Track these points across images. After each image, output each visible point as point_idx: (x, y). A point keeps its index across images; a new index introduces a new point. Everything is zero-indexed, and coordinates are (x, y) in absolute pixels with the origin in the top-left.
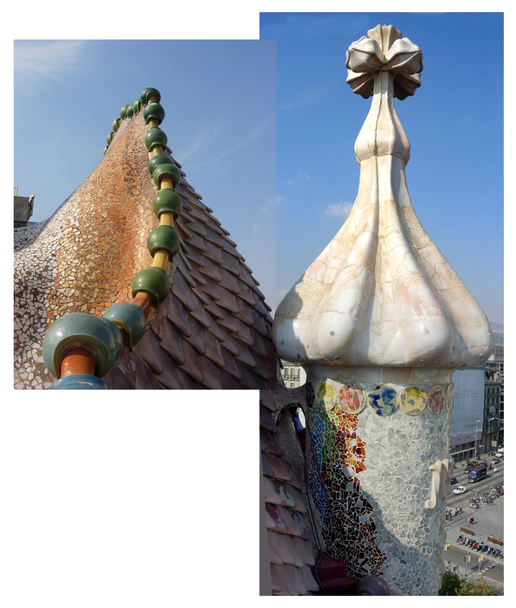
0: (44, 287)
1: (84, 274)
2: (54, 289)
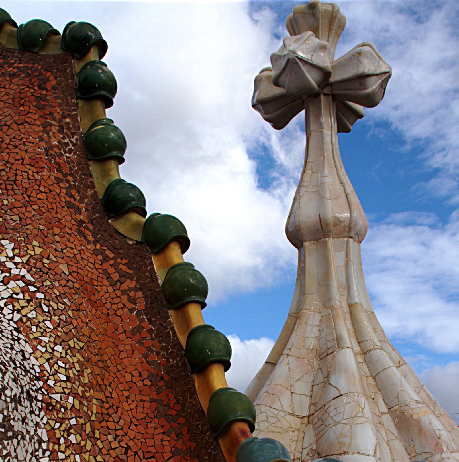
2: (46, 393)
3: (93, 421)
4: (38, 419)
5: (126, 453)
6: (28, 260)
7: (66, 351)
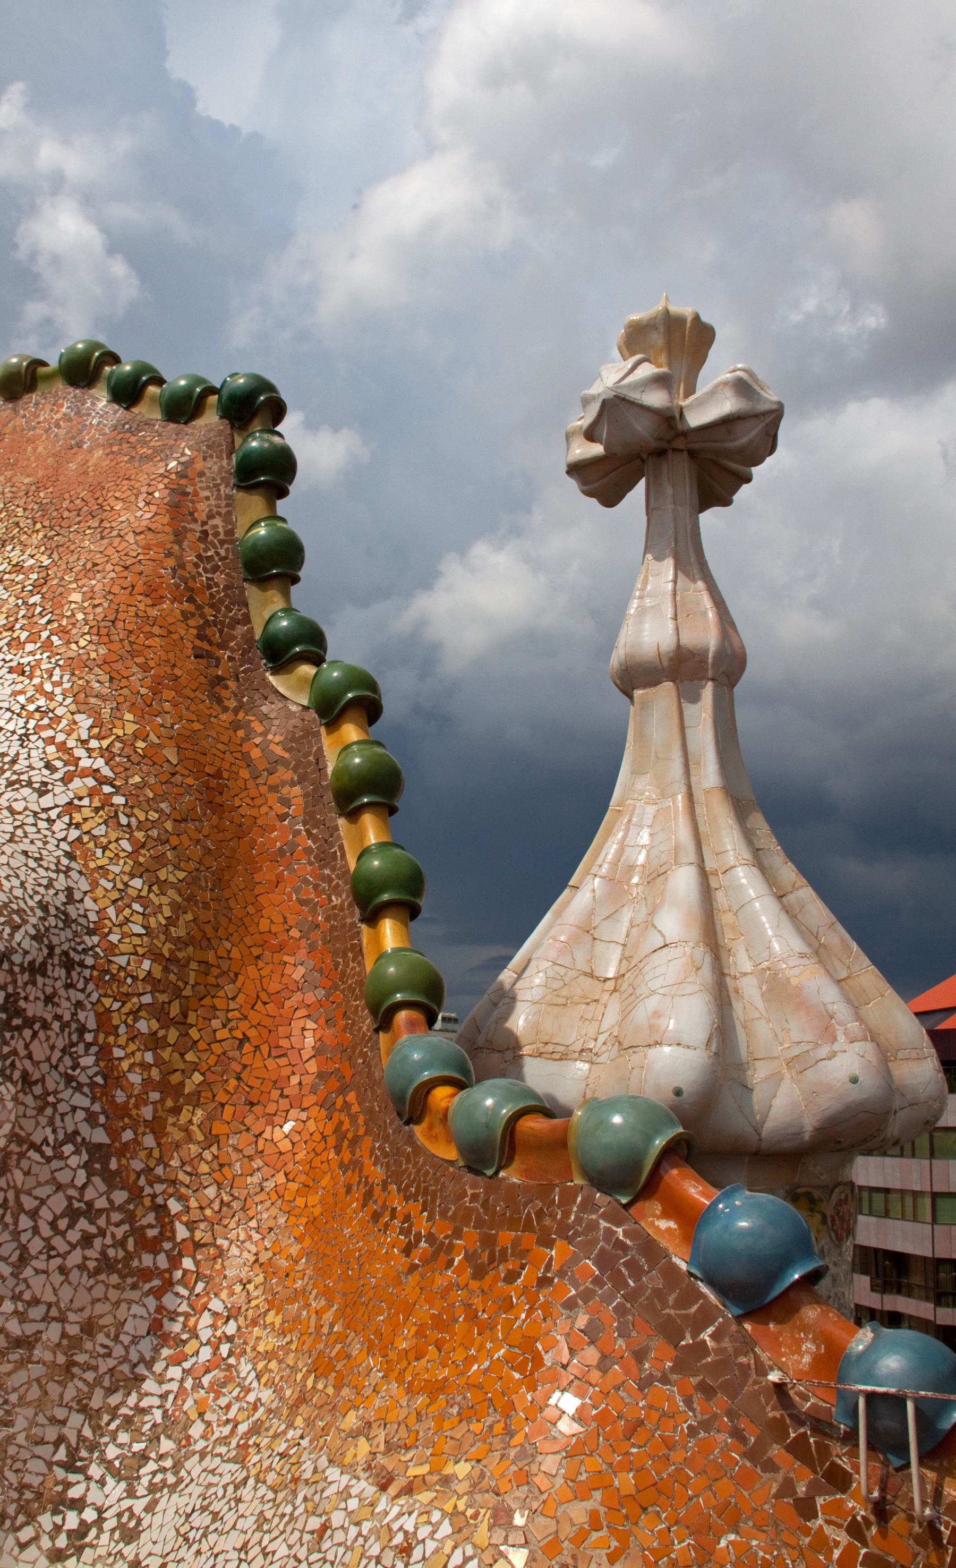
0: (80, 948)
1: (164, 922)
2: (102, 954)
3: (187, 997)
4: (81, 996)
6: (111, 745)
7: (150, 886)
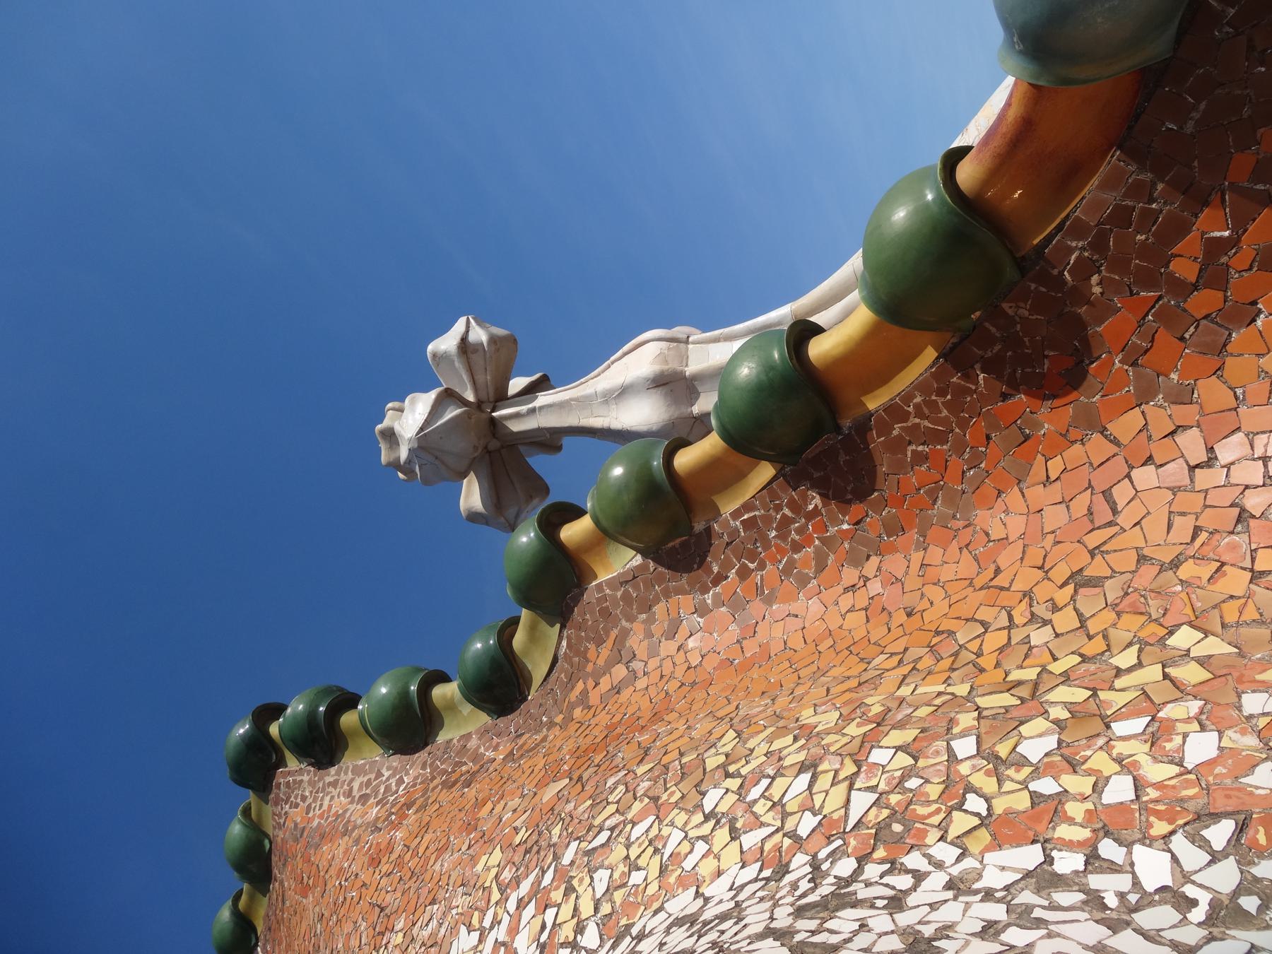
4: (937, 880)
5: (1096, 582)
